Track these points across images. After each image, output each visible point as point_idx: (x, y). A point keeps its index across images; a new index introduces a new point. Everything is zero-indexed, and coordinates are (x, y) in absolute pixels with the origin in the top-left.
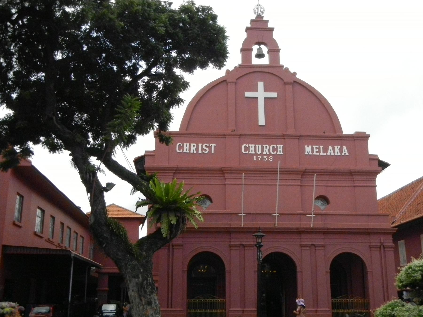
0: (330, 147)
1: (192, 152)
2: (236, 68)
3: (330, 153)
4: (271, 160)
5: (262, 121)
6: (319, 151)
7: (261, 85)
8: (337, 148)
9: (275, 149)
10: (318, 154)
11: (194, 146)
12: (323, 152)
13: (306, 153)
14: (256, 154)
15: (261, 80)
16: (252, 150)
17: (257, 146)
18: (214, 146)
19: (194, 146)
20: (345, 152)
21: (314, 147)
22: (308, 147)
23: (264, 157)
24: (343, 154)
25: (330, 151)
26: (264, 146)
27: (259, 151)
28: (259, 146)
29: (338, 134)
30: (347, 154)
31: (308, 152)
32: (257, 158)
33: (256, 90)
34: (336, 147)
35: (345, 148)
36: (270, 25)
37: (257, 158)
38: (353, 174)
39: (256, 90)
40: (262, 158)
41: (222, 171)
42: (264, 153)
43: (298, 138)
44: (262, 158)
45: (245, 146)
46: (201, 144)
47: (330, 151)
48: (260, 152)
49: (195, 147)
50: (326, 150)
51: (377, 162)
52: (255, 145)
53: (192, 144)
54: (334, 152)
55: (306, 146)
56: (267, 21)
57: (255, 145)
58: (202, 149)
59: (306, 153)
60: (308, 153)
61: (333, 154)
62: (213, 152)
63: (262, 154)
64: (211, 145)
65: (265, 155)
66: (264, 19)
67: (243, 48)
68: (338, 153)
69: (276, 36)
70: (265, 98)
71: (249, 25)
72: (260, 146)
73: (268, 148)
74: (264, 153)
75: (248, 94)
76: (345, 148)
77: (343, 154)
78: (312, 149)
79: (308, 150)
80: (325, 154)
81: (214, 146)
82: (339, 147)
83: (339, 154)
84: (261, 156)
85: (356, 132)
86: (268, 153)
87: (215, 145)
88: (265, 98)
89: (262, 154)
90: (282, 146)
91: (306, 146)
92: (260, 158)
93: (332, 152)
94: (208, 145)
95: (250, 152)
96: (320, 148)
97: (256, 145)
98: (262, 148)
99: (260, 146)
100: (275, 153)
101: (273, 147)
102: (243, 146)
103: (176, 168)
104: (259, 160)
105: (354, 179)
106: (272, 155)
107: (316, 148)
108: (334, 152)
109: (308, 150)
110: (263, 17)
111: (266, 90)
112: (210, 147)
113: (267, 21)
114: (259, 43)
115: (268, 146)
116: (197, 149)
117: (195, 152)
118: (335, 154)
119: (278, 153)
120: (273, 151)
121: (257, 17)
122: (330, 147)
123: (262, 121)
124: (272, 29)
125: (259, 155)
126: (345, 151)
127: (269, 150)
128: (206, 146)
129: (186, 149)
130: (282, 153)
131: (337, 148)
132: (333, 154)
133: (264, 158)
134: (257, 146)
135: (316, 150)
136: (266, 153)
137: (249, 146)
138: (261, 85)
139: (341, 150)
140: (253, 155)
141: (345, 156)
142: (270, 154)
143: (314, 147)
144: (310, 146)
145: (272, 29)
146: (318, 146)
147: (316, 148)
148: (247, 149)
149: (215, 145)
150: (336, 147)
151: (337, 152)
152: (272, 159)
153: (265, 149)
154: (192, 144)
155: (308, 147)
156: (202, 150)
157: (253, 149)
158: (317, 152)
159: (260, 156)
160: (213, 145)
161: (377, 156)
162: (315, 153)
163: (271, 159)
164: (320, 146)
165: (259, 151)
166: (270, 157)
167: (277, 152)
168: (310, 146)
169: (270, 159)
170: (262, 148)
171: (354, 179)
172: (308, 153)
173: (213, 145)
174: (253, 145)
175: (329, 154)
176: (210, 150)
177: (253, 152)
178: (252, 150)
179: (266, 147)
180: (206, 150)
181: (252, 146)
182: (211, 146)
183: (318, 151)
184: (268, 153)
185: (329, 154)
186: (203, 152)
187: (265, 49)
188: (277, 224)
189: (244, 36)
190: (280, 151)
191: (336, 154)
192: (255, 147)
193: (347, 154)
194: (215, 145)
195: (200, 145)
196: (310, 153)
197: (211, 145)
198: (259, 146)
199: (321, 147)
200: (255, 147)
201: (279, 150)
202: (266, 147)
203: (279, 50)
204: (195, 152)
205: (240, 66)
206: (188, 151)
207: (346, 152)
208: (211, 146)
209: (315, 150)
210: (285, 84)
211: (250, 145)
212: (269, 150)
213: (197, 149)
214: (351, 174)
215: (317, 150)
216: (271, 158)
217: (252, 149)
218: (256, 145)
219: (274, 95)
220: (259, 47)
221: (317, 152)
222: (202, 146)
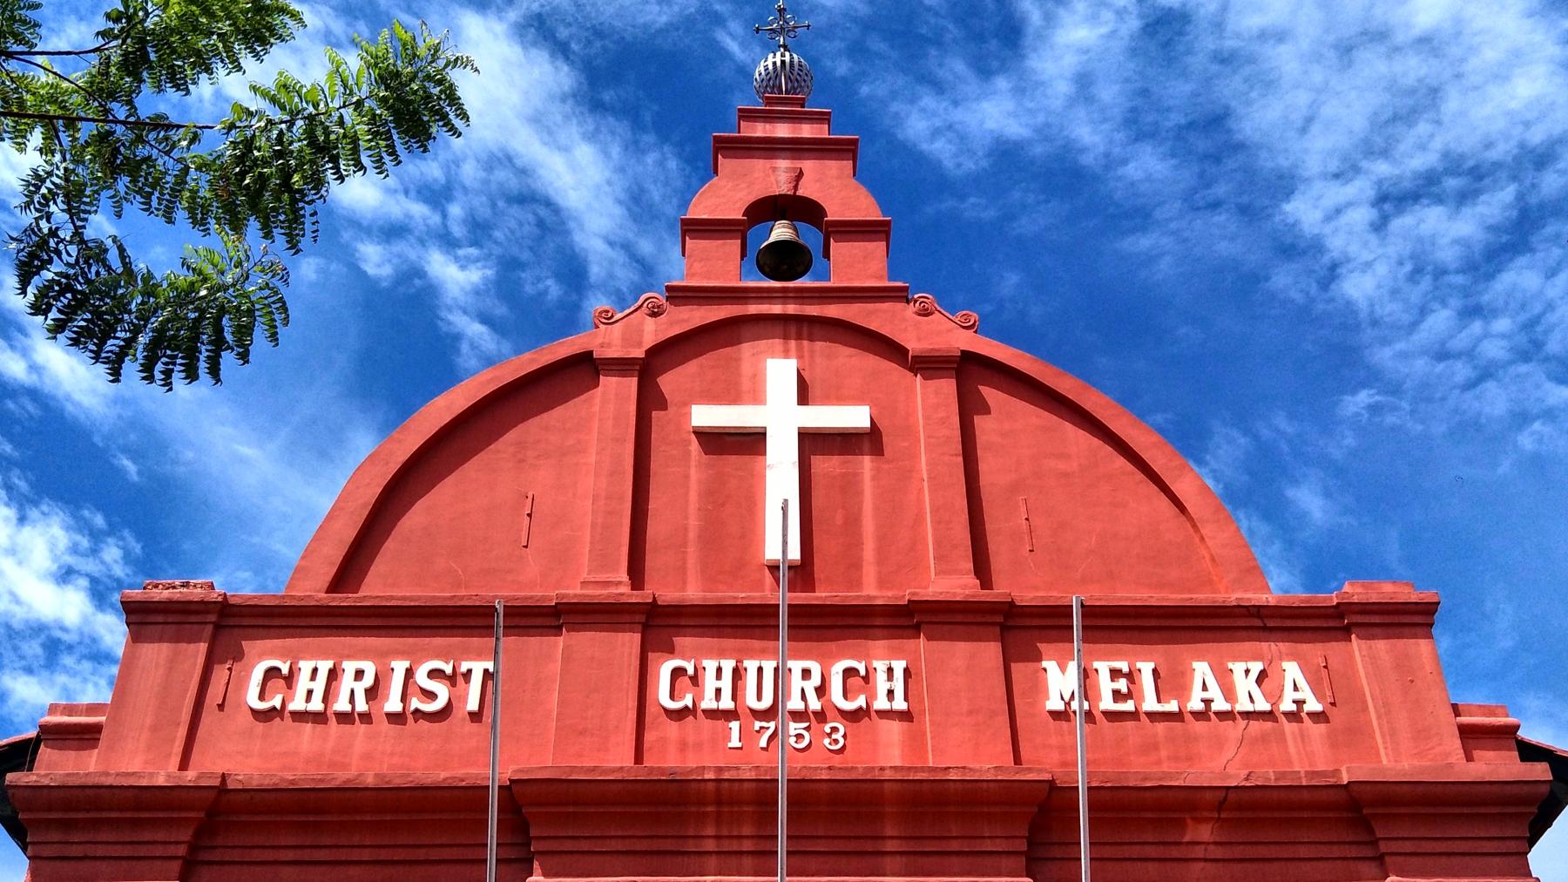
0: (1201, 669)
1: (342, 705)
3: (1207, 702)
4: (836, 741)
8: (1247, 672)
10: (1129, 706)
11: (359, 674)
16: (718, 691)
17: (751, 665)
18: (486, 671)
19: (359, 674)
21: (1103, 667)
22: (1063, 668)
23: (794, 728)
24: (1287, 705)
25: (1205, 688)
26: (796, 666)
27: (759, 697)
28: (760, 670)
30: (1313, 705)
31: (1067, 698)
33: (756, 396)
34: (1238, 668)
38: (1365, 811)
43: (1000, 619)
46: (406, 664)
47: (1205, 688)
48: (767, 702)
49: (368, 680)
52: (739, 661)
53: (350, 667)
54: (1229, 693)
55: (1050, 665)
57: (739, 661)
59: (1055, 704)
60: (1068, 704)
61: (1226, 707)
62: (473, 704)
65: (797, 716)
68: (1252, 701)
73: (816, 680)
74: (795, 704)
75: (706, 416)
76: (1292, 670)
78: (1087, 676)
80: (1172, 706)
81: (486, 671)
82: (1256, 667)
83: (1262, 705)
84: (772, 725)
87: (491, 670)
90: (899, 666)
91: (1050, 665)
92: (769, 732)
93: (1215, 692)
94: (448, 669)
95: (708, 703)
96: (1131, 676)
97: (746, 663)
99: (769, 666)
100: (861, 701)
101: (849, 673)
102: (666, 669)
103: (212, 795)
104: (763, 743)
105: (1384, 847)
107: (1115, 674)
111: (804, 396)
115: (815, 668)
117: (362, 706)
118: (1238, 708)
119: (881, 703)
122: (1201, 669)
126: (1296, 688)
127: (821, 691)
128: (434, 674)
129: (310, 692)
130: (900, 704)
131: (1247, 672)
132: (1220, 705)
133: (793, 732)
134: (751, 665)
135: (1116, 685)
136: (800, 706)
138: (780, 372)
143: (1103, 667)
144: (1072, 667)
146: (1124, 666)
147: (1115, 674)
150: (1238, 668)
151: (1248, 694)
152: (838, 736)
153: (796, 682)
154: (350, 667)
155: (1063, 668)
156: (404, 698)
157: (726, 684)
158: (1117, 696)
159: (764, 724)
160: (478, 667)
162: (1107, 703)
164: (1139, 665)
165: (759, 697)
166: (828, 730)
167: (871, 697)
169: (827, 741)
171: (1384, 847)
172: (1068, 704)
173: (478, 667)
174: (728, 665)
175: (1195, 704)
177: (727, 703)
178: (715, 690)
179: (806, 674)
180: (431, 696)
181: (719, 670)
182: (470, 671)
183: (1124, 690)
184: (815, 704)
185: (1200, 706)
186: (415, 703)
190: (890, 693)
191: (1243, 705)
192: (738, 674)
194: (490, 666)
197: (464, 666)
198: (760, 670)
199: (1146, 668)
200: (738, 674)
201: (882, 685)
202: (806, 674)
204: (362, 706)
206: (316, 705)
207: (1306, 693)
208: (470, 671)
209: (1106, 686)
211: (710, 665)
212: (821, 691)
215: (1122, 684)
216: (835, 729)
217: (718, 684)
218: (746, 663)
219: (856, 417)
221: (1117, 696)
222: (409, 673)
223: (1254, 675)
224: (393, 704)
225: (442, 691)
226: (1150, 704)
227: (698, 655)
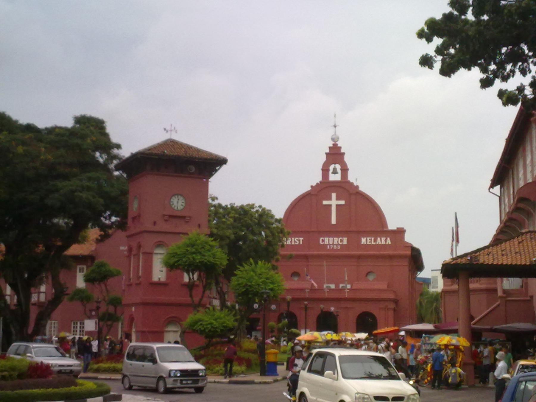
0: (379, 239)
2: (317, 183)
5: (334, 221)
6: (371, 242)
7: (334, 195)
9: (342, 241)
10: (370, 243)
12: (374, 242)
13: (362, 243)
14: (329, 244)
15: (334, 192)
17: (330, 238)
20: (389, 242)
24: (387, 243)
27: (331, 242)
29: (385, 229)
30: (390, 243)
32: (330, 247)
35: (388, 239)
36: (342, 151)
37: (330, 247)
39: (330, 199)
40: (333, 247)
41: (306, 257)
42: (335, 243)
44: (333, 247)
45: (322, 239)
48: (332, 243)
50: (375, 241)
51: (410, 249)
54: (381, 242)
56: (340, 148)
58: (295, 242)
59: (362, 243)
62: (301, 243)
63: (333, 244)
64: (300, 238)
65: (335, 245)
66: (339, 145)
67: (324, 168)
69: (346, 159)
70: (337, 205)
71: (328, 151)
72: (332, 239)
74: (335, 243)
75: (325, 202)
76: (388, 239)
77: (387, 243)
78: (367, 240)
79: (363, 240)
80: (375, 243)
82: (385, 238)
83: (385, 243)
85: (398, 228)
86: (337, 243)
88: (337, 205)
89: (333, 244)
91: (362, 238)
93: (380, 241)
95: (326, 243)
96: (371, 240)
98: (333, 240)
99: (332, 239)
101: (341, 240)
106: (340, 245)
107: (369, 239)
108: (381, 242)
109: (363, 240)
110: (337, 145)
111: (338, 199)
112: (299, 240)
113: (340, 148)
114: (335, 164)
116: (291, 242)
120: (341, 242)
121: (333, 145)
122: (379, 239)
123: (334, 221)
124: (344, 154)
125: (332, 245)
127: (338, 242)
128: (297, 240)
132: (380, 243)
137: (325, 239)
138: (334, 195)
139: (386, 241)
140: (328, 245)
141: (388, 245)
142: (338, 244)
143: (368, 239)
144: (365, 238)
145: (344, 154)
148: (323, 241)
149: (302, 239)
151: (383, 242)
155: (364, 238)
160: (301, 239)
161: (410, 244)
162: (368, 243)
163: (339, 247)
168: (365, 238)
170: (333, 240)
173: (301, 239)
175: (377, 243)
176: (299, 242)
177: (328, 243)
178: (326, 242)
180: (297, 242)
184: (337, 243)
187: (338, 167)
188: (326, 295)
189: (324, 158)
191: (383, 243)
193: (390, 243)
195: (293, 239)
196: (365, 243)
199: (373, 239)
202: (336, 240)
203: (348, 170)
205: (321, 182)
209: (368, 241)
210: (350, 194)
211: (326, 238)
212: (338, 242)
213: (291, 242)
214: (391, 257)
215: (370, 241)
219: (342, 202)
220: (335, 166)
223: (384, 239)
224: (293, 243)
225: (297, 241)
226: (373, 243)
227: (324, 237)
